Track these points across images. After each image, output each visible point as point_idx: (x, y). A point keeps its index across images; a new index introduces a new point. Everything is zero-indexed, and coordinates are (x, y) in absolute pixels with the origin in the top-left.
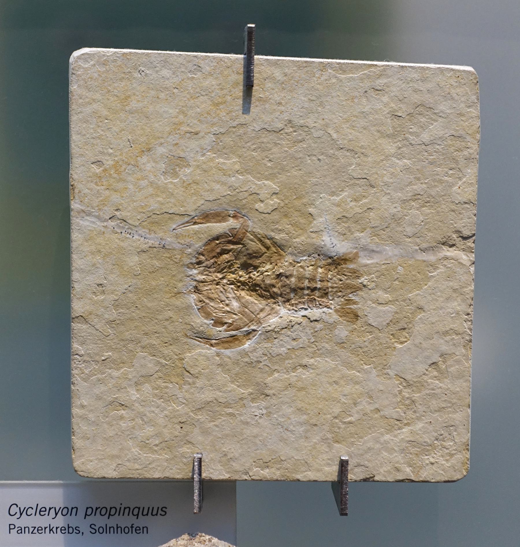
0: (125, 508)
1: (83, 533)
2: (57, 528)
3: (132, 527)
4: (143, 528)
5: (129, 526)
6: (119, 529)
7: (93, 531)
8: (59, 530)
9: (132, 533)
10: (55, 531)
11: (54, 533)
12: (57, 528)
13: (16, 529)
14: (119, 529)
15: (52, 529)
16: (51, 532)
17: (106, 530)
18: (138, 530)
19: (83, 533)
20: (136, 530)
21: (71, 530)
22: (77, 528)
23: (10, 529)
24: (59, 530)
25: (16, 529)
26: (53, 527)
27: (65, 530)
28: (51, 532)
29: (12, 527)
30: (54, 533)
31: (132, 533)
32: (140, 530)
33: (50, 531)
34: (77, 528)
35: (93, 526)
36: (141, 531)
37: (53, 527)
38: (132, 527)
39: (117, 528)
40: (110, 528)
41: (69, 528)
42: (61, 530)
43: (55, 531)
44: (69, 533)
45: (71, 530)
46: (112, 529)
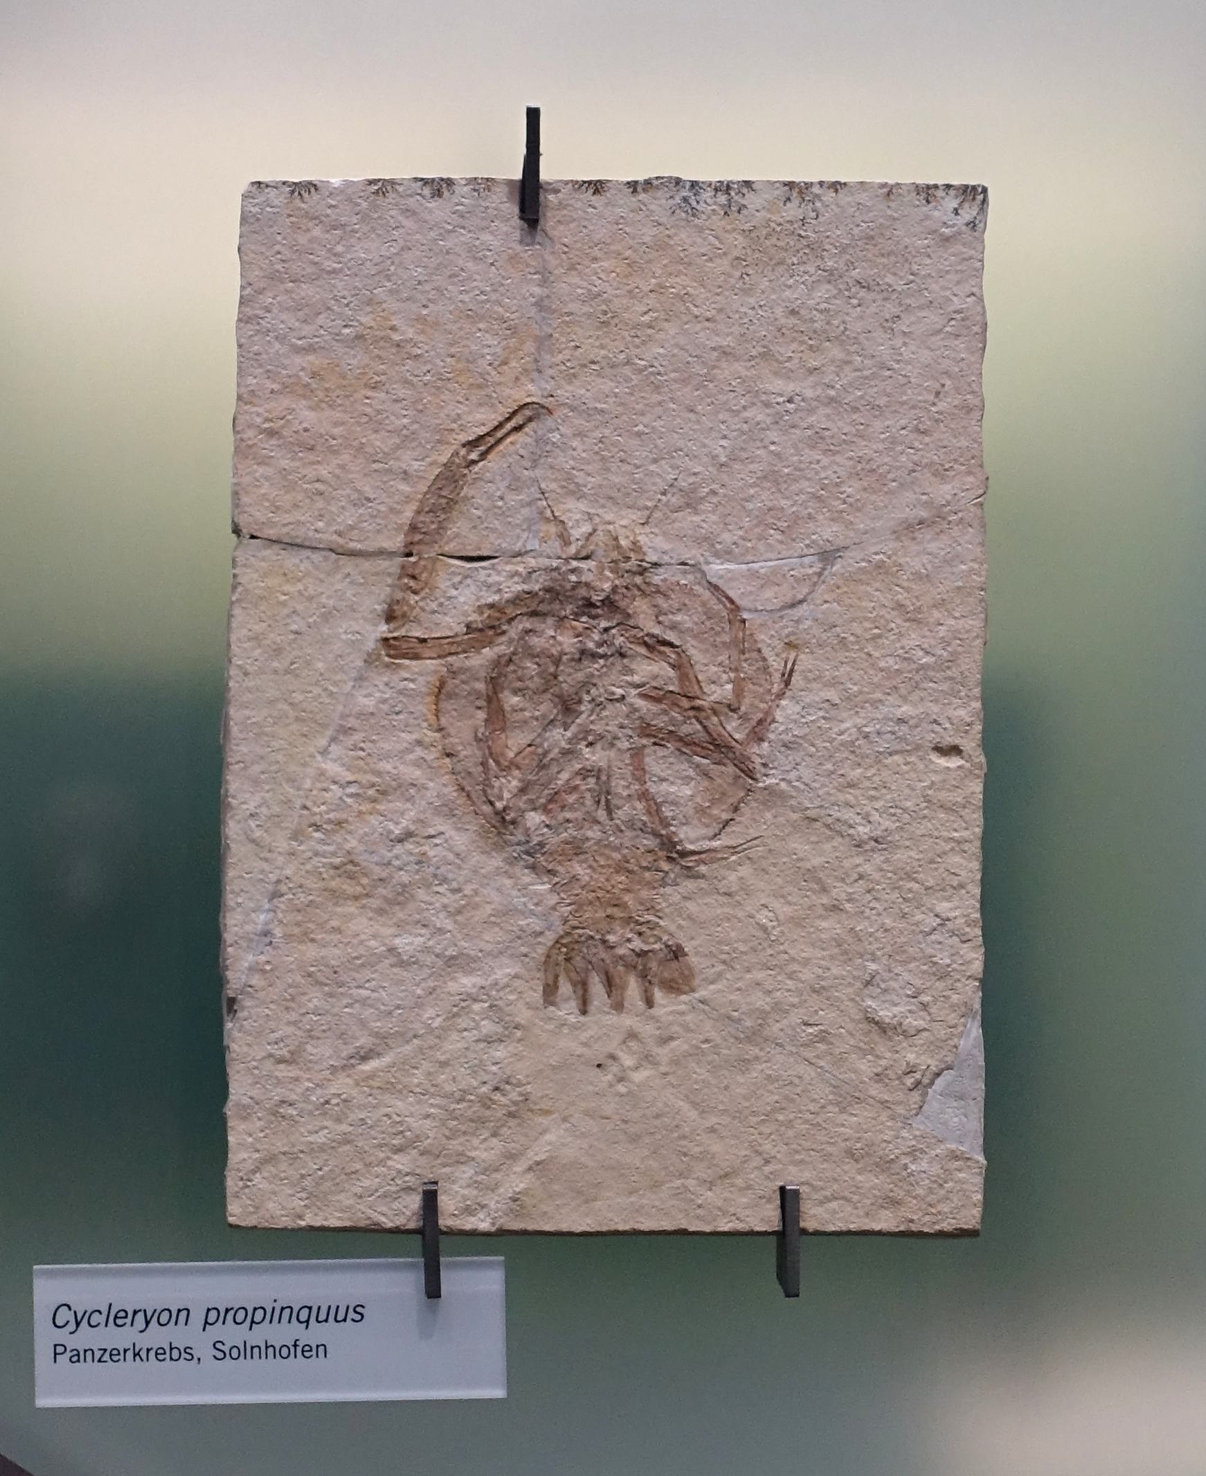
0: (283, 1309)
1: (199, 1359)
2: (148, 1350)
3: (295, 1346)
4: (318, 1346)
5: (290, 1344)
6: (271, 1350)
7: (220, 1355)
8: (152, 1353)
9: (296, 1357)
10: (144, 1357)
11: (142, 1360)
12: (148, 1350)
13: (69, 1354)
14: (271, 1350)
15: (138, 1354)
16: (137, 1358)
17: (247, 1351)
18: (307, 1351)
19: (199, 1359)
20: (303, 1351)
21: (175, 1354)
22: (188, 1350)
23: (56, 1354)
24: (152, 1353)
25: (69, 1354)
26: (140, 1350)
27: (165, 1353)
28: (137, 1358)
29: (60, 1349)
30: (142, 1360)
31: (296, 1357)
32: (311, 1351)
33: (135, 1355)
34: (188, 1350)
35: (219, 1346)
36: (314, 1352)
37: (140, 1350)
38: (295, 1346)
39: (267, 1347)
40: (252, 1348)
41: (171, 1349)
42: (157, 1354)
43: (144, 1357)
44: (171, 1359)
45: (175, 1354)
46: (256, 1350)
